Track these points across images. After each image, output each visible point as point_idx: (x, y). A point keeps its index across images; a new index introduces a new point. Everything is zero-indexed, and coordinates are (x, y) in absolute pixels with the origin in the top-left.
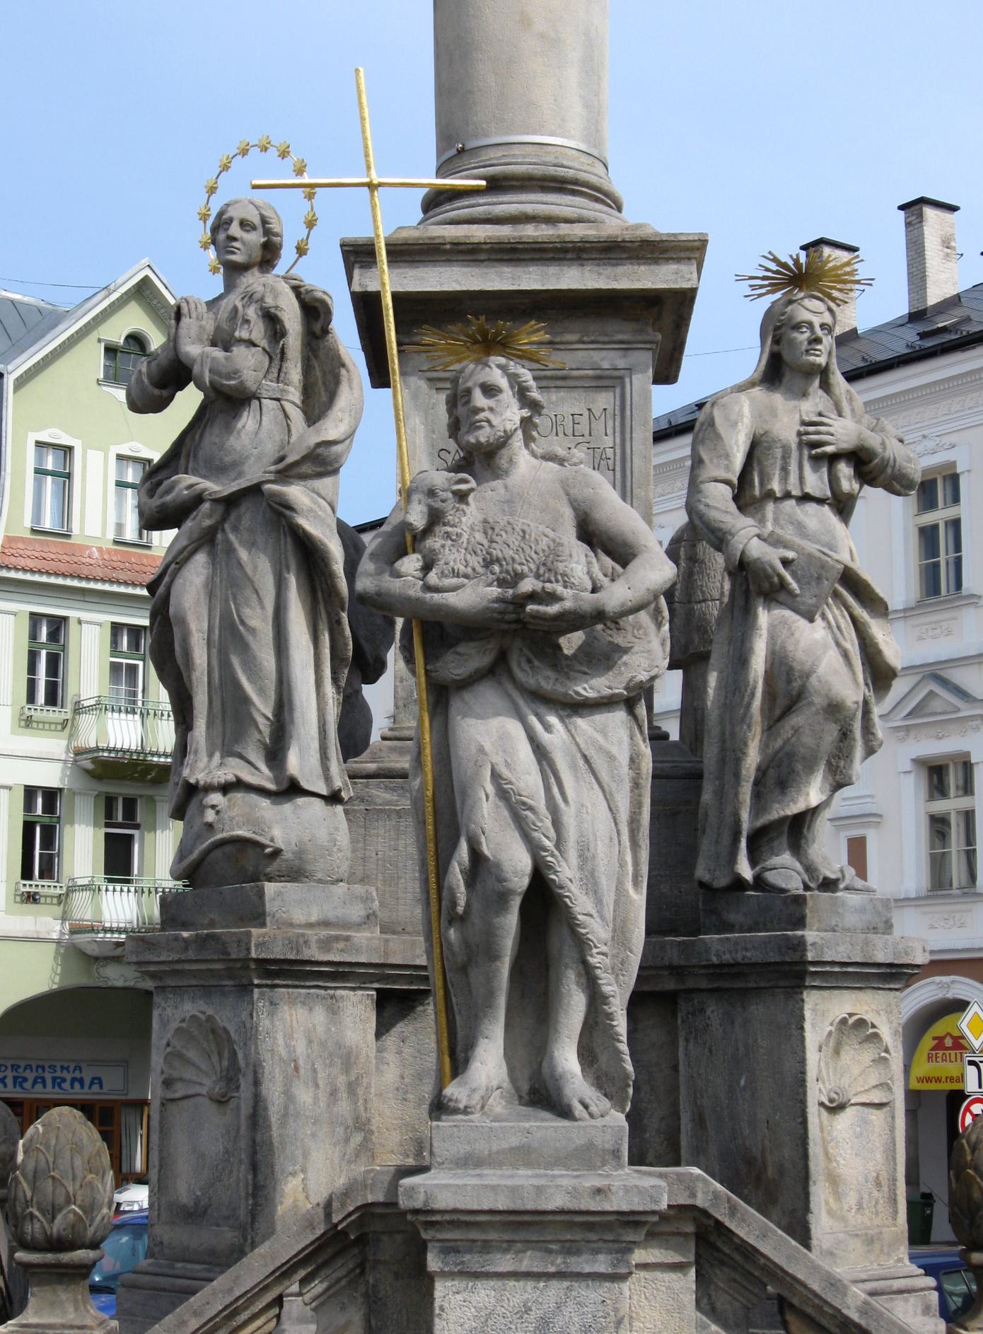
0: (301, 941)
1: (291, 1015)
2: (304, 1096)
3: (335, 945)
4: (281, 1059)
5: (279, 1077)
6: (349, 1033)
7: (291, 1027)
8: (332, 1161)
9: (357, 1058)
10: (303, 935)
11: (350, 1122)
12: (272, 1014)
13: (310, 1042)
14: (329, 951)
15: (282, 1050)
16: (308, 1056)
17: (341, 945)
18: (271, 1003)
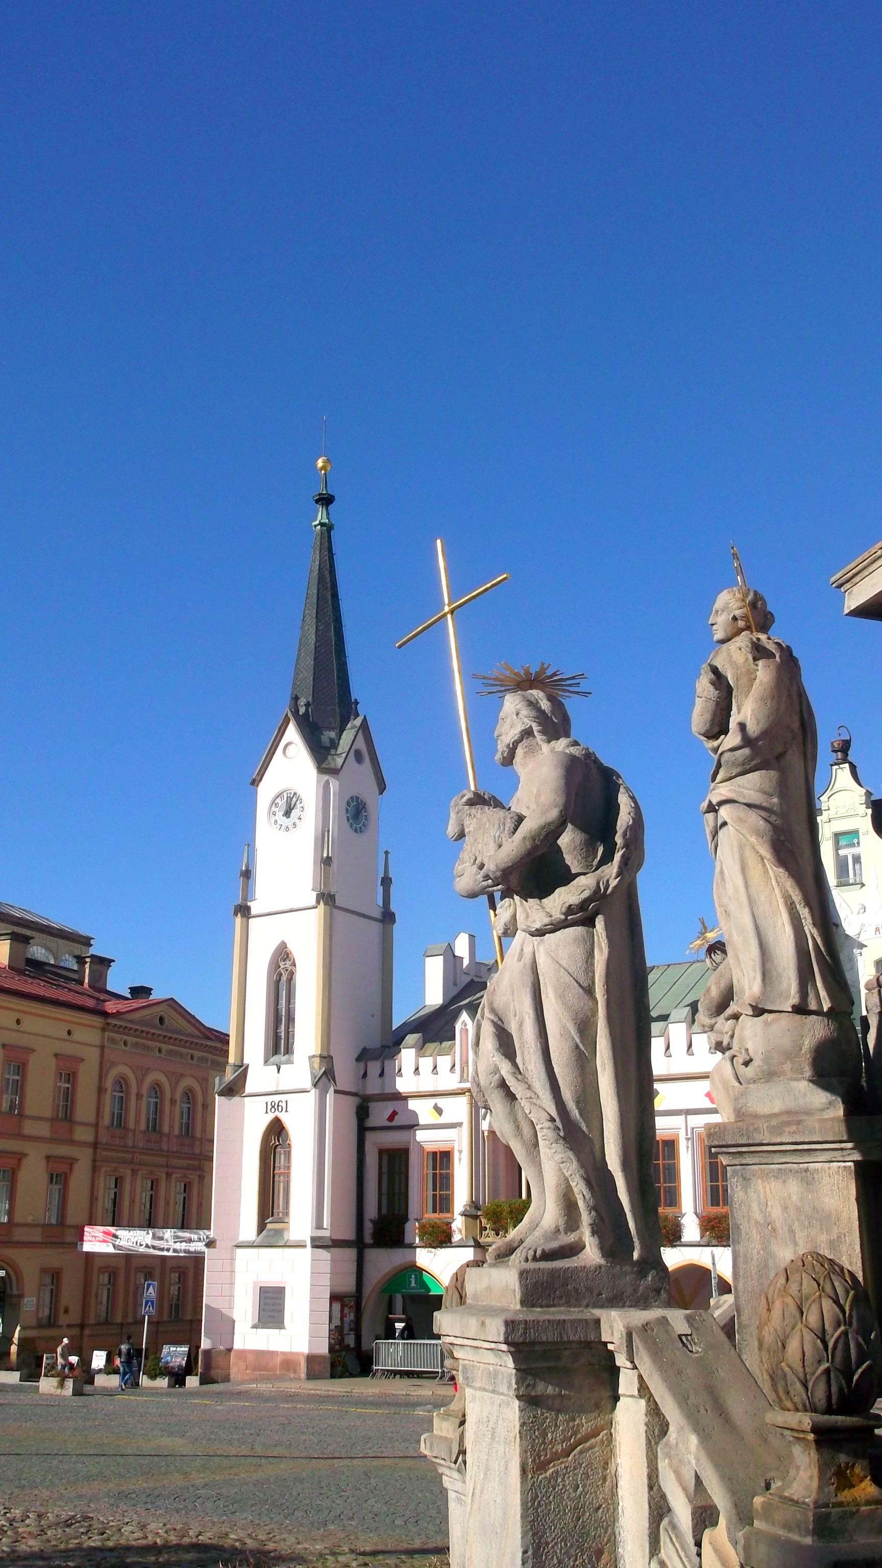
0: (751, 1128)
1: (764, 1187)
3: (787, 1129)
4: (757, 1223)
5: (756, 1236)
6: (827, 1200)
7: (765, 1197)
10: (753, 1124)
12: (745, 1188)
13: (785, 1209)
14: (781, 1134)
15: (757, 1215)
16: (785, 1220)
17: (794, 1128)
18: (744, 1179)
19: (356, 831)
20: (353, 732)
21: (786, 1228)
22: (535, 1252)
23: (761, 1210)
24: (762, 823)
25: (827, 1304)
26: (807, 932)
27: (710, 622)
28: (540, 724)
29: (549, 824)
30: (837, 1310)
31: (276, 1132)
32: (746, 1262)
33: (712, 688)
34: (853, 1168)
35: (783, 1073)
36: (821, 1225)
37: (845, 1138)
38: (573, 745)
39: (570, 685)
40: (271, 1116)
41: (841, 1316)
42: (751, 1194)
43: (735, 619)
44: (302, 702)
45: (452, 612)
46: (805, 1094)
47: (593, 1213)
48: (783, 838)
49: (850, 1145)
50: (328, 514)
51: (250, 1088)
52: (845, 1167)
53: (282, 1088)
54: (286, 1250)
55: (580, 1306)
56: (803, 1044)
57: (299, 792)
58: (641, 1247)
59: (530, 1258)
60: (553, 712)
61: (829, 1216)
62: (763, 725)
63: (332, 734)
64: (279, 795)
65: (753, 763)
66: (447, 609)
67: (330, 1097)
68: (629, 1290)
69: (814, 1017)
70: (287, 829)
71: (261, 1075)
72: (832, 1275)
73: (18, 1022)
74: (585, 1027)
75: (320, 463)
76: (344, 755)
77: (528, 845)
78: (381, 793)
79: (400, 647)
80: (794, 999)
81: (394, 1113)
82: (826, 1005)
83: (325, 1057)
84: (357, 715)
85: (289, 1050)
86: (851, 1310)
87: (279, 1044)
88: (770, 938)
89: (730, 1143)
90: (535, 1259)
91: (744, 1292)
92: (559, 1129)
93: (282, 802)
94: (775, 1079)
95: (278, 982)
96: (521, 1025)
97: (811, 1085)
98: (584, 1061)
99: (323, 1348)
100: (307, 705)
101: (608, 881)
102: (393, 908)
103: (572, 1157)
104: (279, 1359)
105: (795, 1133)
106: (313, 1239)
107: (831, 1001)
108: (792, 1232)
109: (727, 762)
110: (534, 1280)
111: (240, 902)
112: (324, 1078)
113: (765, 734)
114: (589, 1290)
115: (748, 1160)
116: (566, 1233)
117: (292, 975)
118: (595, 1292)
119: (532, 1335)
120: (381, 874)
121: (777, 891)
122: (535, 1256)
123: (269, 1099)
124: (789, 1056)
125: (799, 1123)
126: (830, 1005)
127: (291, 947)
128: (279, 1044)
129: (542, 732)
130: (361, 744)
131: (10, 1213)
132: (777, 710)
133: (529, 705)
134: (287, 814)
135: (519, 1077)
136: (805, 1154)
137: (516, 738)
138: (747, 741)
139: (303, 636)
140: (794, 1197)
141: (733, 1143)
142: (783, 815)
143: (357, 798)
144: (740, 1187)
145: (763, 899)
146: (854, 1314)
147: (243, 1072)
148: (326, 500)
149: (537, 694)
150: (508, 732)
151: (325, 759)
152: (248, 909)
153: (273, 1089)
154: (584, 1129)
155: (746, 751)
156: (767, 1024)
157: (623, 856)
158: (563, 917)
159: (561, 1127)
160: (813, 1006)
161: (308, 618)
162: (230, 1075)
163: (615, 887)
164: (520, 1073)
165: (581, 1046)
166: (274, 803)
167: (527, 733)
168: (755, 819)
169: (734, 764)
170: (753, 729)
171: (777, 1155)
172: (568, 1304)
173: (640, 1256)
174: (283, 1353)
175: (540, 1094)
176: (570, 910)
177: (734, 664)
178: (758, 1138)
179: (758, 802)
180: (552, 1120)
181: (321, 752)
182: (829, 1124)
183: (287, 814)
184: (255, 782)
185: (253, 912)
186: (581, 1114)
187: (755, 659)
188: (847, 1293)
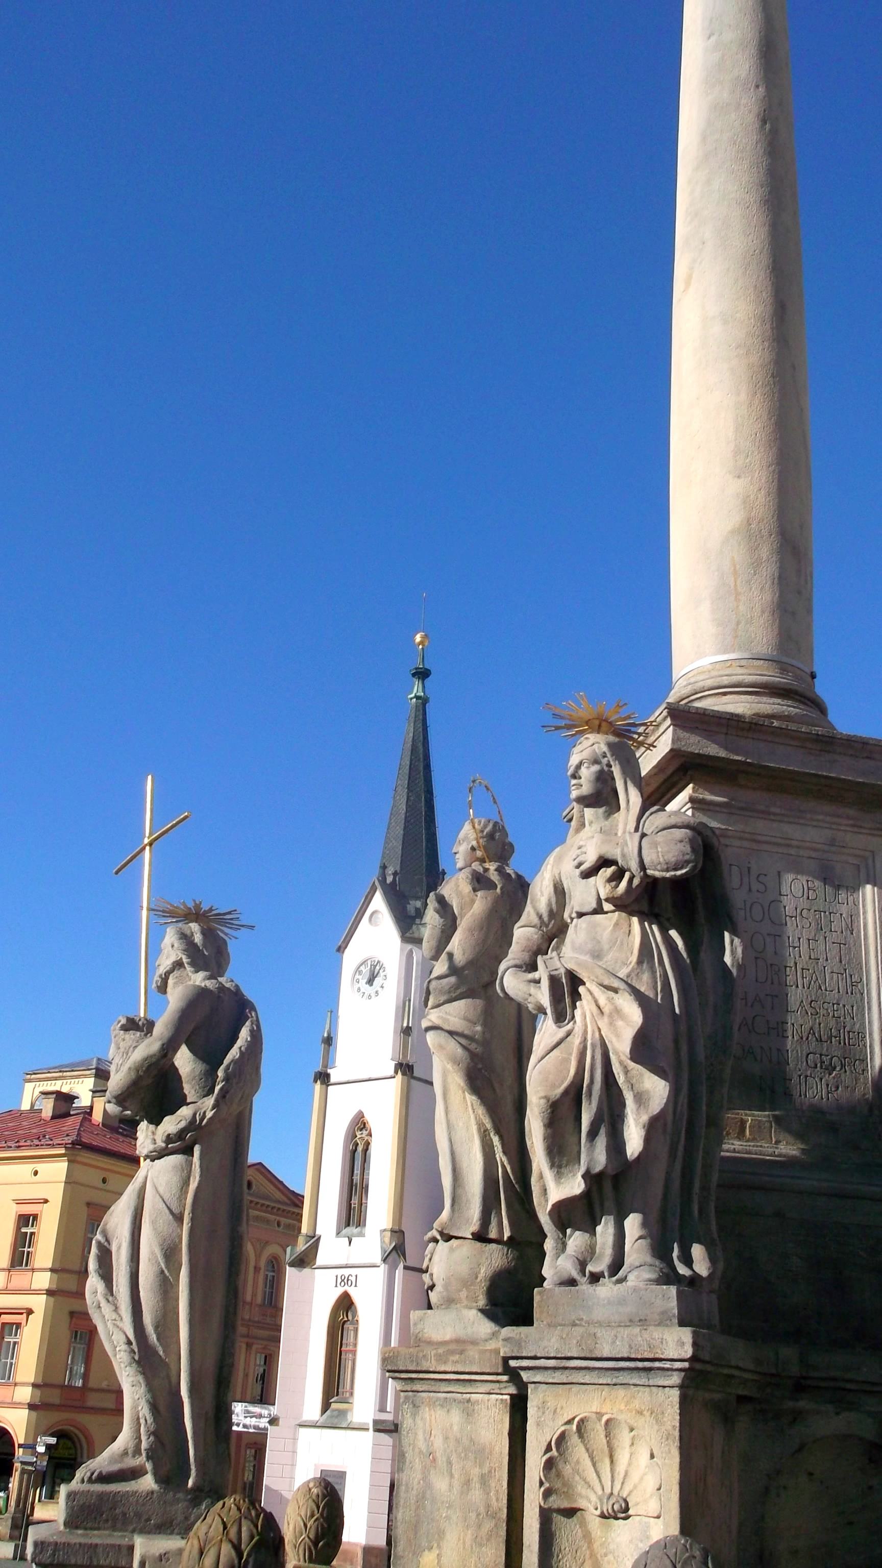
2: (441, 1484)
4: (421, 1452)
5: (418, 1465)
6: (483, 1432)
8: (464, 1543)
9: (491, 1453)
11: (482, 1509)
12: (414, 1415)
13: (446, 1438)
15: (421, 1444)
16: (445, 1451)
17: (457, 1357)
18: (414, 1406)
21: (444, 1459)
22: (92, 1474)
23: (425, 1439)
24: (460, 1050)
25: (226, 1549)
26: (498, 1159)
27: (454, 851)
28: (189, 956)
29: (151, 1056)
30: (233, 1553)
31: (345, 1306)
32: (407, 1491)
33: (437, 916)
34: (509, 1401)
35: (459, 1301)
36: (476, 1458)
37: (500, 1370)
38: (208, 979)
39: (231, 919)
40: (340, 1291)
41: (236, 1562)
42: (419, 1421)
43: (473, 849)
44: (390, 871)
45: (151, 844)
46: (473, 1323)
47: (152, 1438)
48: (480, 1066)
49: (505, 1378)
50: (424, 687)
51: (320, 1260)
52: (502, 1400)
53: (351, 1262)
54: (349, 1432)
55: (126, 1531)
56: (479, 1273)
57: (382, 960)
58: (197, 1475)
59: (86, 1480)
60: (204, 945)
61: (482, 1450)
62: (469, 955)
63: (418, 904)
64: (364, 963)
65: (459, 991)
66: (146, 841)
67: (399, 1272)
68: (180, 1517)
69: (494, 1246)
70: (370, 997)
71: (332, 1248)
72: (244, 1521)
73: (104, 1181)
74: (170, 1253)
75: (418, 638)
77: (133, 1075)
79: (117, 873)
80: (474, 1225)
82: (507, 1234)
83: (396, 1232)
86: (249, 1555)
87: (352, 1216)
88: (464, 1164)
89: (401, 1368)
90: (90, 1480)
91: (402, 1523)
92: (135, 1353)
93: (365, 970)
94: (453, 1306)
95: (354, 1151)
96: (119, 1248)
97: (479, 1314)
98: (166, 1287)
100: (395, 874)
101: (205, 1113)
103: (142, 1381)
105: (457, 1362)
106: (375, 1422)
107: (511, 1230)
108: (450, 1463)
109: (435, 989)
110: (81, 1502)
111: (319, 1068)
112: (394, 1253)
113: (471, 964)
114: (138, 1515)
115: (418, 1386)
116: (134, 1456)
117: (368, 1144)
118: (145, 1517)
119: (61, 1557)
121: (472, 1117)
122: (90, 1478)
123: (340, 1272)
124: (467, 1283)
125: (462, 1352)
126: (509, 1234)
127: (368, 1117)
128: (352, 1216)
129: (191, 964)
131: (85, 1377)
132: (484, 941)
133: (181, 938)
134: (370, 982)
135: (110, 1299)
136: (467, 1384)
137: (168, 968)
138: (454, 970)
139: (394, 806)
140: (455, 1428)
141: (404, 1369)
142: (485, 1043)
144: (409, 1414)
145: (461, 1124)
146: (251, 1560)
147: (315, 1242)
148: (422, 674)
149: (195, 927)
150: (165, 962)
151: (410, 927)
152: (328, 1076)
153: (343, 1262)
154: (161, 1353)
155: (452, 979)
156: (452, 1250)
157: (221, 1089)
158: (164, 1145)
159: (136, 1350)
160: (493, 1234)
161: (399, 789)
162: (302, 1245)
163: (211, 1118)
164: (112, 1295)
165: (166, 1272)
166: (358, 971)
167: (178, 964)
168: (454, 1047)
169: (441, 992)
170: (460, 958)
171: (443, 1384)
172: (114, 1528)
173: (194, 1484)
175: (124, 1317)
176: (169, 1139)
177: (459, 894)
178: (425, 1366)
179: (460, 1030)
180: (129, 1343)
181: (407, 922)
182: (488, 1354)
183: (370, 982)
184: (341, 949)
185: (332, 1080)
186: (158, 1339)
187: (475, 890)
188: (252, 1537)
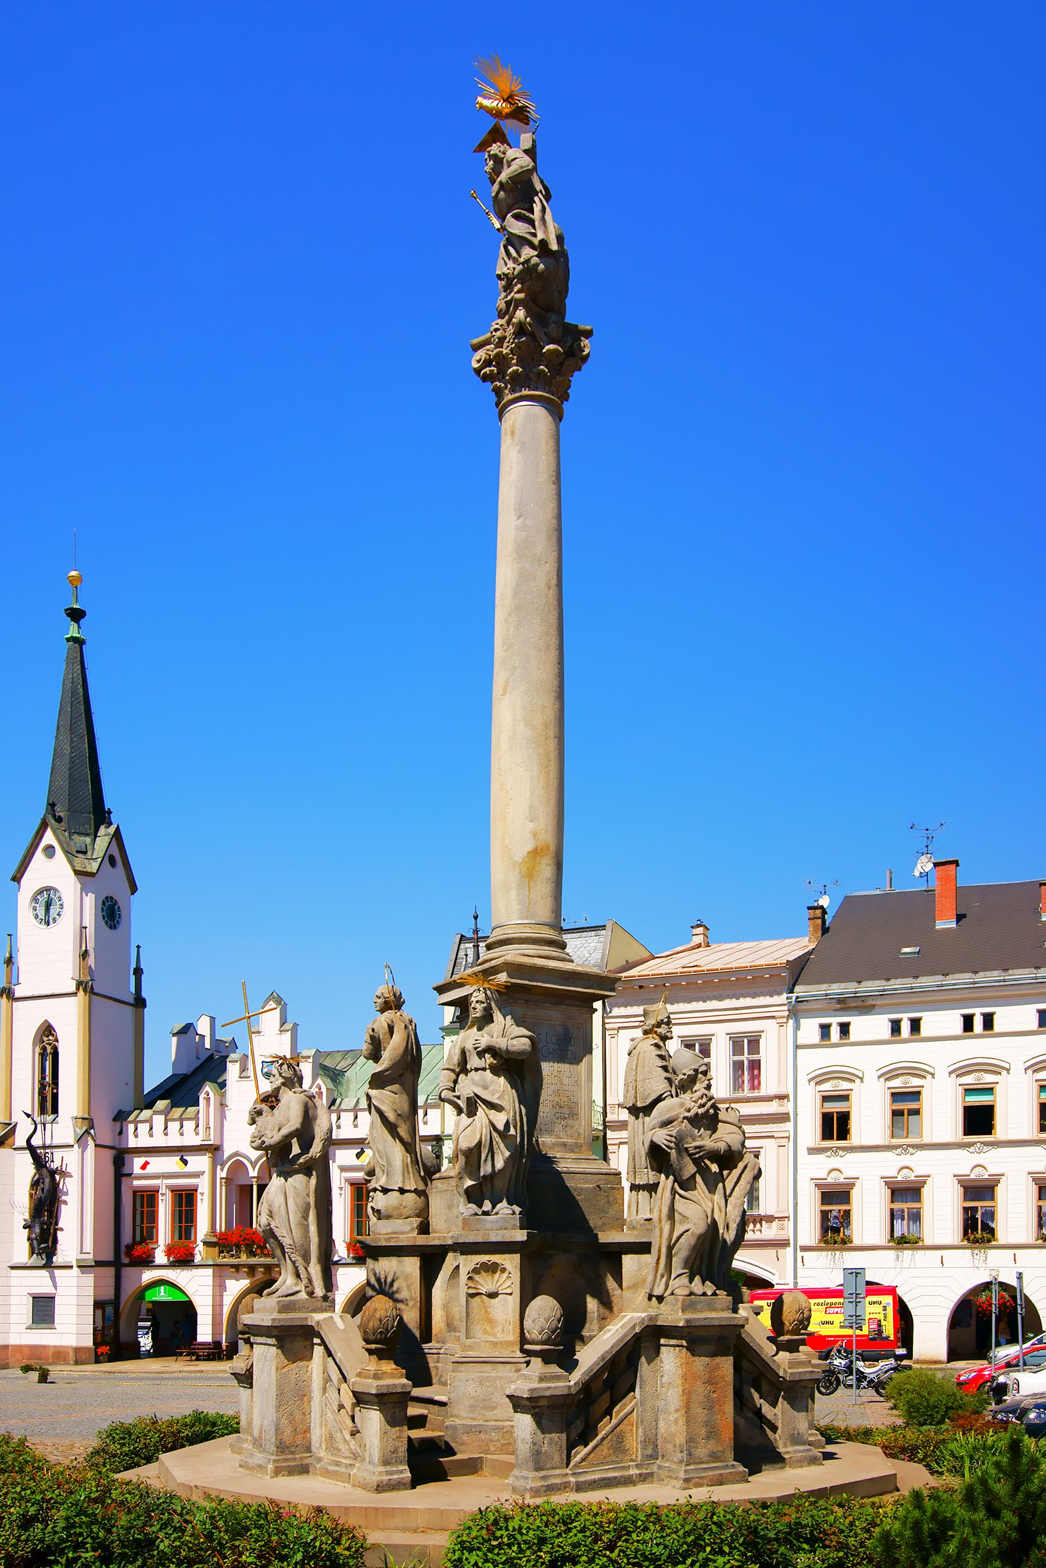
19: (111, 928)
20: (107, 839)
50: (79, 627)
76: (99, 860)
78: (133, 894)
81: (146, 1163)
84: (110, 824)
85: (55, 1110)
99: (88, 1342)
102: (144, 994)
104: (51, 1351)
120: (133, 965)
130: (115, 851)
143: (112, 898)
161: (62, 729)
174: (55, 1347)
